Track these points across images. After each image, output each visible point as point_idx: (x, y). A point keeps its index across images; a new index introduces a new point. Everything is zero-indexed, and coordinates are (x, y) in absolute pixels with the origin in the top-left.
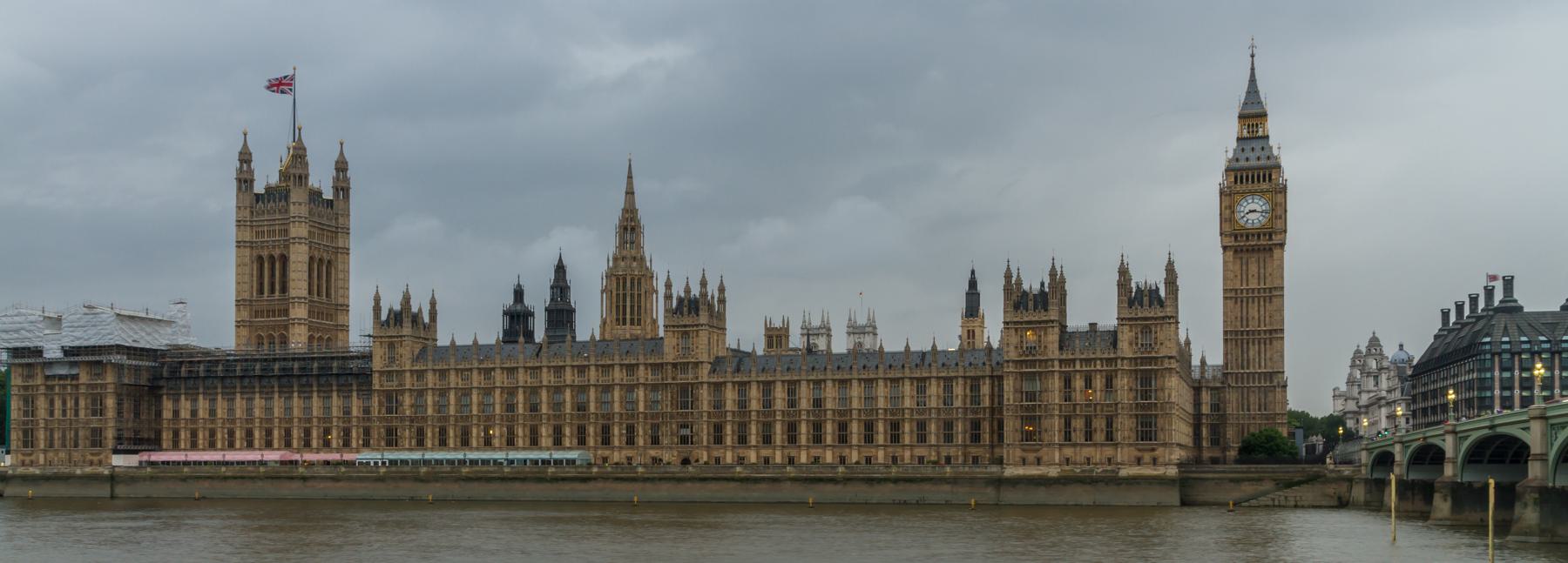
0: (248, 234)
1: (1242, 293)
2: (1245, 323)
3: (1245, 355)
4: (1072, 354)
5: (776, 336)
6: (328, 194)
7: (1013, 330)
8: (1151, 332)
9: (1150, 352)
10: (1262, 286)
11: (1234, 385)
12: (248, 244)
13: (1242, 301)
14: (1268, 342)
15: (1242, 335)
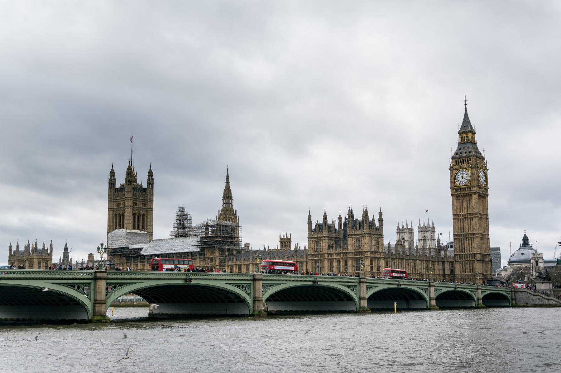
0: (112, 205)
1: (460, 216)
2: (462, 230)
3: (463, 246)
4: (333, 251)
5: (285, 242)
6: (145, 186)
7: (311, 241)
8: (360, 240)
9: (359, 250)
10: (469, 212)
11: (459, 260)
12: (112, 210)
13: (461, 220)
14: (472, 239)
15: (461, 236)
